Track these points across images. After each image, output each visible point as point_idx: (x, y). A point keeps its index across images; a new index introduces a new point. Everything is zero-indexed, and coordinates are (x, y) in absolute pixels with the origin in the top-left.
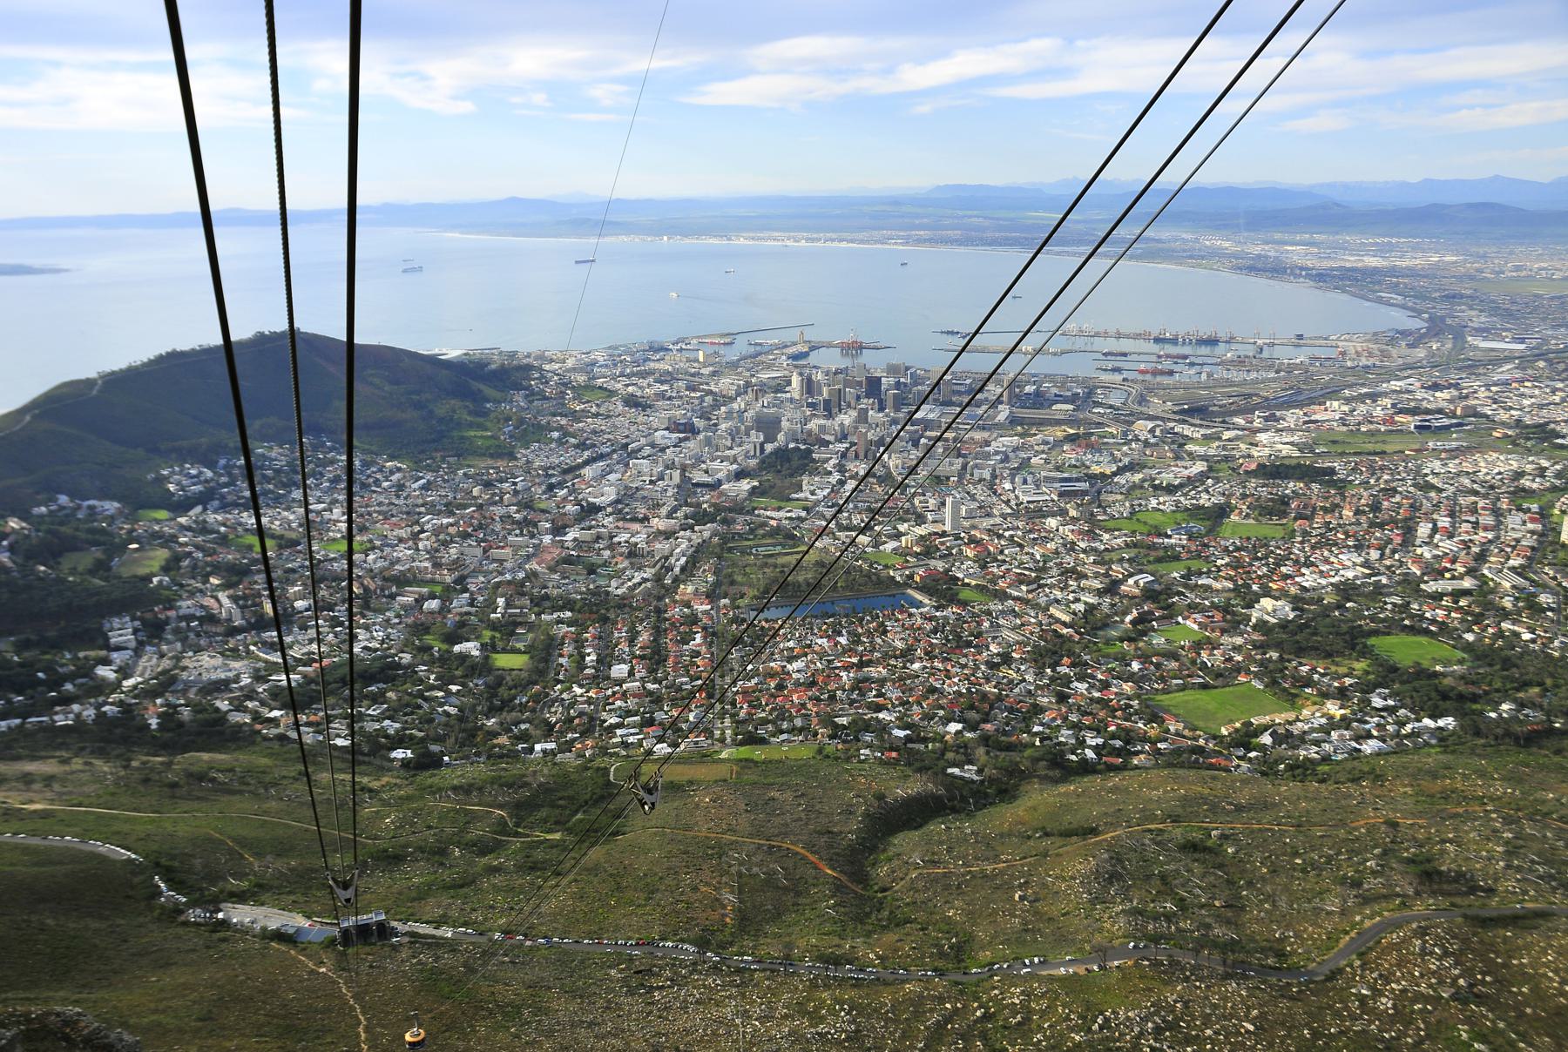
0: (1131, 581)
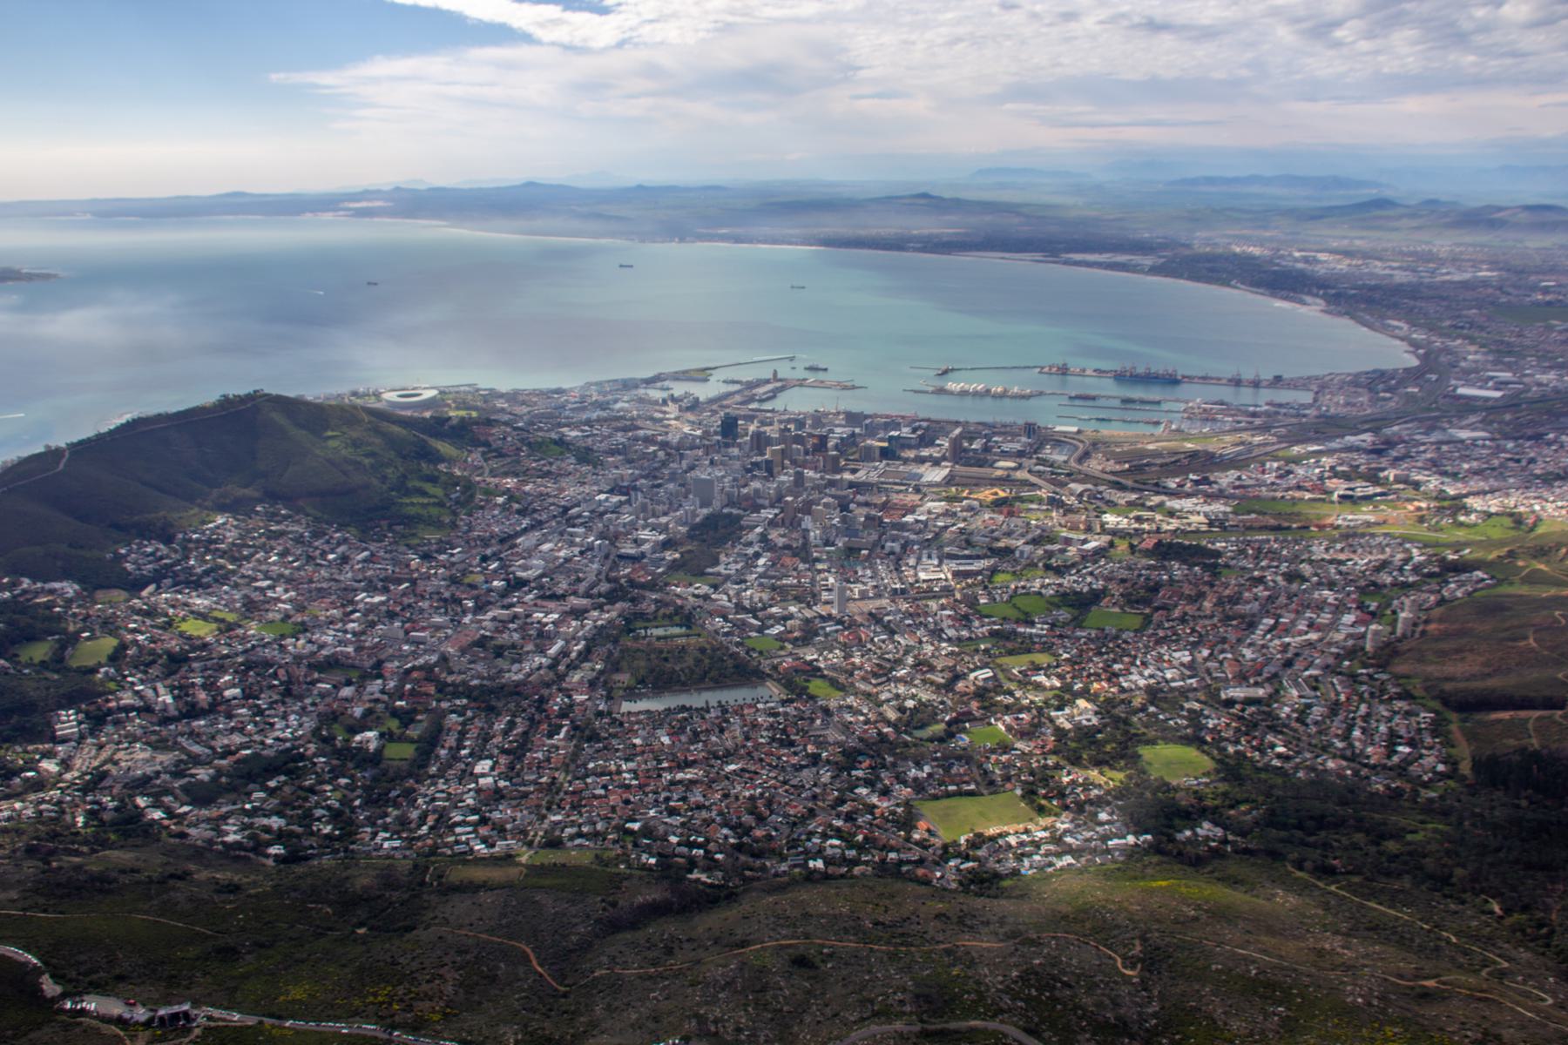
0: (972, 676)
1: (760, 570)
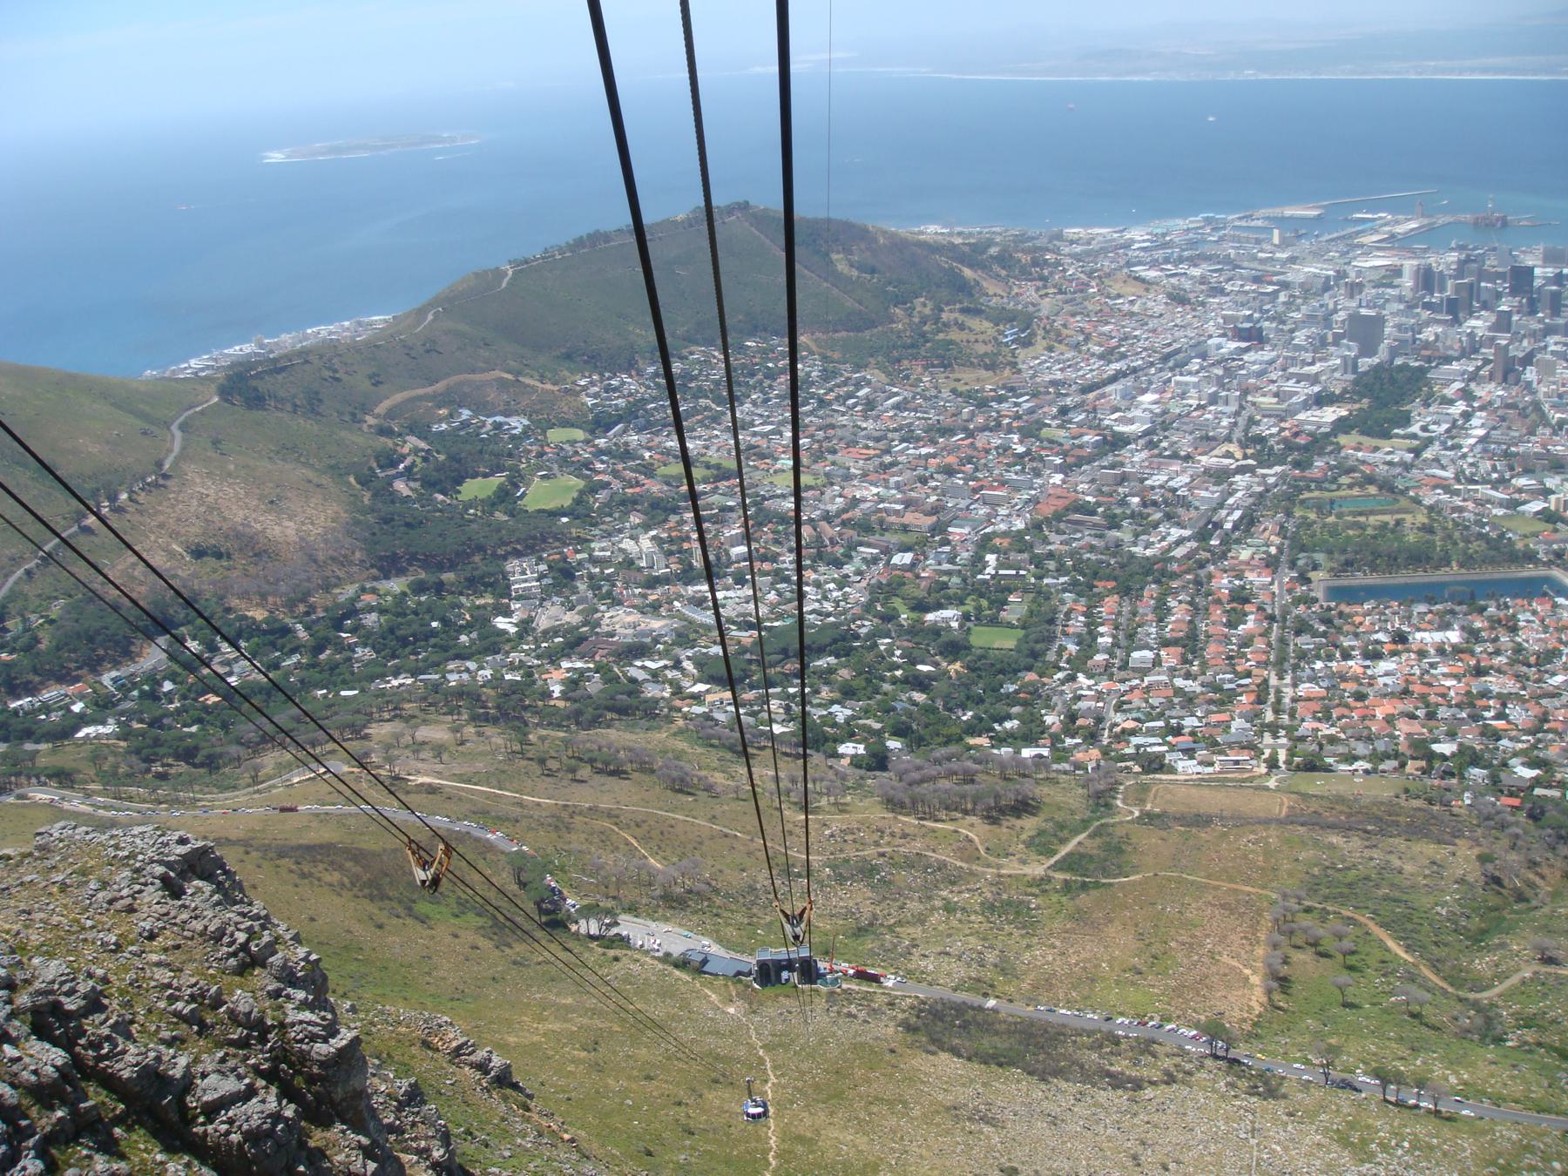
1: (1481, 432)
